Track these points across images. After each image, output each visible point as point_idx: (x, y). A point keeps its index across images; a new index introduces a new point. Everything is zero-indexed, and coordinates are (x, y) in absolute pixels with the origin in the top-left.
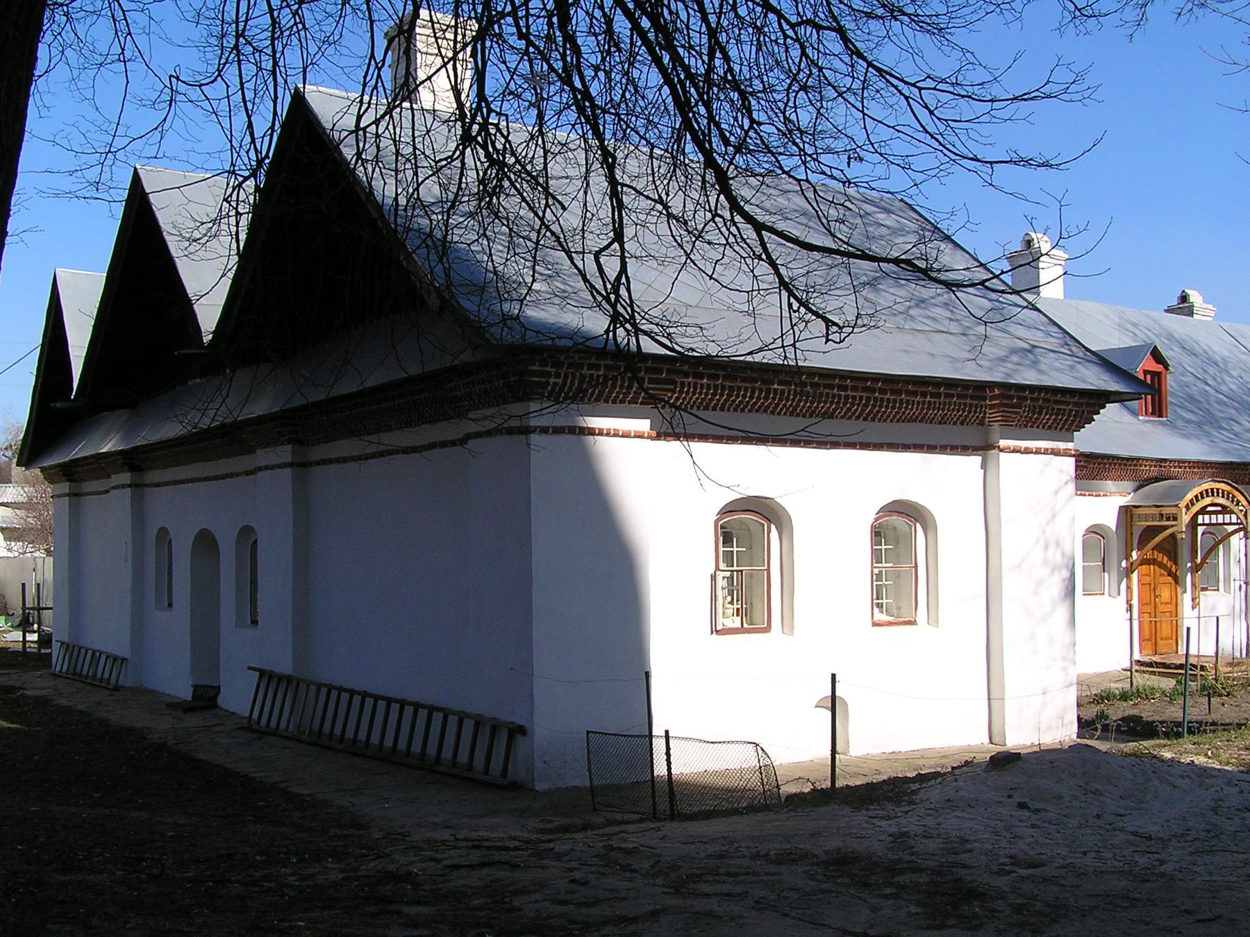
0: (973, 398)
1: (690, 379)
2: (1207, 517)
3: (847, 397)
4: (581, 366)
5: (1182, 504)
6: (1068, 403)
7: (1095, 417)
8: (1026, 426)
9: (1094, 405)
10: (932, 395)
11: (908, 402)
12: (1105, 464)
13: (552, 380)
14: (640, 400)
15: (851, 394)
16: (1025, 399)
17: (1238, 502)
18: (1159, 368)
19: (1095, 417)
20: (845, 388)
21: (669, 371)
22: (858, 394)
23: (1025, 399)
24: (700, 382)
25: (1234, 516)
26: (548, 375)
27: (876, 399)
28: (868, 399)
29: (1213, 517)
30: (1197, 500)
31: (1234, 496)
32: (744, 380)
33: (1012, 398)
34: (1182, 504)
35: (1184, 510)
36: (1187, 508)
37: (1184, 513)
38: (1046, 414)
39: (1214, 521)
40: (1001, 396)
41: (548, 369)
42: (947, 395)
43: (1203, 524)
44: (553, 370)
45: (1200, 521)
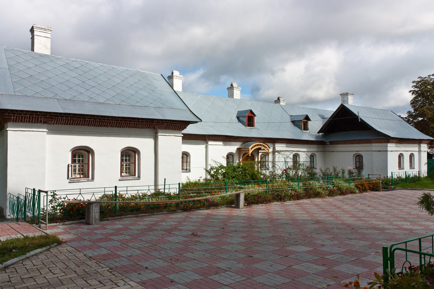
0: (150, 122)
1: (64, 118)
2: (261, 151)
3: (110, 122)
4: (21, 114)
5: (250, 148)
6: (178, 124)
7: (187, 127)
8: (166, 129)
9: (185, 124)
10: (137, 122)
11: (130, 123)
12: (232, 138)
13: (12, 117)
14: (39, 121)
15: (111, 121)
16: (164, 123)
17: (266, 148)
18: (252, 115)
19: (187, 127)
20: (109, 120)
21: (49, 116)
22: (114, 121)
23: (164, 123)
24: (63, 118)
25: (265, 151)
26: (11, 116)
27: (119, 123)
28: (117, 123)
29: (262, 151)
30: (254, 147)
31: (265, 146)
32: (76, 118)
33: (160, 122)
34: (250, 148)
35: (250, 149)
36: (252, 148)
37: (250, 150)
38: (171, 126)
39: (264, 152)
40: (157, 122)
41: (11, 114)
42: (141, 122)
43: (260, 152)
44: (12, 115)
45: (260, 152)
